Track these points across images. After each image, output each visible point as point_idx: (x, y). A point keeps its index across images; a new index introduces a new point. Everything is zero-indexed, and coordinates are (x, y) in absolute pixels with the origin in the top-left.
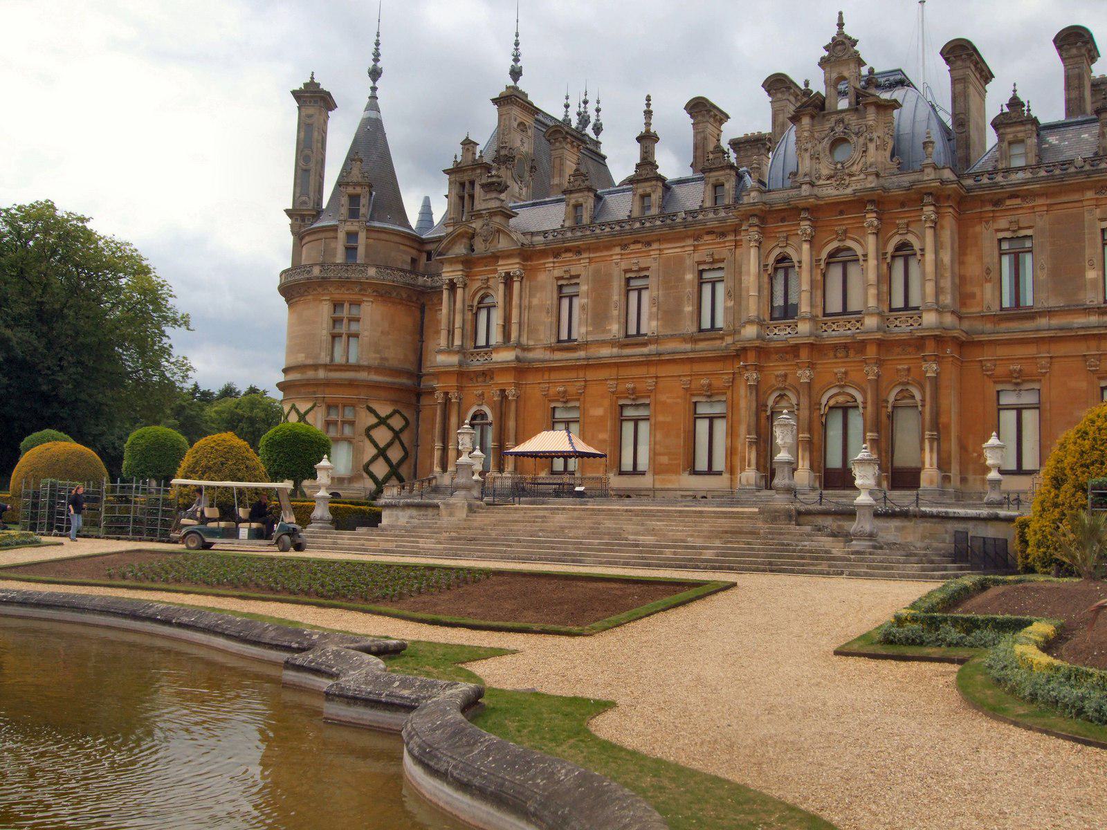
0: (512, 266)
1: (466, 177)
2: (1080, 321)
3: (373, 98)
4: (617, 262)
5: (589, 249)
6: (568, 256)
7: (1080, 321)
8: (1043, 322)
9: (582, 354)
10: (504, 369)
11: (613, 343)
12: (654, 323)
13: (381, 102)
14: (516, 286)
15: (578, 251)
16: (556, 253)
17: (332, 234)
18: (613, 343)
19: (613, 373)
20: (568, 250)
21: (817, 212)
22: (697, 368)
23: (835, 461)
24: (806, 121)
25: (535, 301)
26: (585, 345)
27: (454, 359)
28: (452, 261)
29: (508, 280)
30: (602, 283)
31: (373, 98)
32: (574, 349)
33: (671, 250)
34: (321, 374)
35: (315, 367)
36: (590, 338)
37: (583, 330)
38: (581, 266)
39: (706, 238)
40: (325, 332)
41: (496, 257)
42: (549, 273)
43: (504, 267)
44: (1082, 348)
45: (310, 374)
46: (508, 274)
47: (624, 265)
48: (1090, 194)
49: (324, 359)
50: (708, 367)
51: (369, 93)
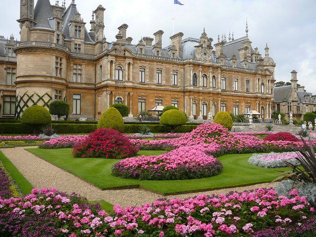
0: (131, 61)
1: (78, 25)
2: (232, 93)
4: (155, 66)
5: (150, 61)
7: (232, 93)
8: (228, 93)
10: (129, 88)
11: (155, 85)
12: (164, 82)
14: (131, 66)
15: (146, 61)
16: (140, 60)
18: (155, 85)
19: (155, 92)
20: (143, 60)
21: (204, 66)
22: (174, 93)
23: (205, 115)
24: (200, 48)
25: (134, 71)
26: (148, 84)
27: (114, 83)
28: (112, 55)
29: (129, 64)
30: (151, 70)
32: (145, 85)
33: (168, 66)
34: (53, 80)
35: (52, 77)
36: (149, 83)
37: (148, 80)
38: (146, 65)
39: (175, 65)
40: (54, 66)
41: (125, 58)
42: (139, 64)
43: (128, 61)
44: (232, 97)
45: (49, 79)
47: (157, 67)
48: (233, 73)
49: (54, 75)
50: (176, 93)
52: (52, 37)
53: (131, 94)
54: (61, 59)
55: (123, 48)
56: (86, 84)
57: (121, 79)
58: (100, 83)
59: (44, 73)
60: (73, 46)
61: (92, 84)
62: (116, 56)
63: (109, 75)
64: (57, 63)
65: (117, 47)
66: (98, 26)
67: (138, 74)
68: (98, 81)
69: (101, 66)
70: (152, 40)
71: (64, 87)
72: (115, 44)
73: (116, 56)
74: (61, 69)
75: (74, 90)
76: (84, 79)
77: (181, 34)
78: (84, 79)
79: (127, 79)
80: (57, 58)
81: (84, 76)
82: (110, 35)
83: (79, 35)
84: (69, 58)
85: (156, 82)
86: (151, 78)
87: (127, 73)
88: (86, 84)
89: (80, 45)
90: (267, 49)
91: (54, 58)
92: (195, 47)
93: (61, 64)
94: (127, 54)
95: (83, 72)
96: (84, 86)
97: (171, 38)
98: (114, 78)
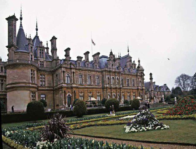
3: (21, 24)
5: (84, 70)
6: (81, 71)
9: (84, 86)
13: (23, 25)
14: (75, 74)
15: (82, 70)
17: (28, 54)
18: (87, 85)
28: (64, 67)
30: (85, 76)
31: (21, 24)
34: (30, 85)
35: (29, 83)
38: (83, 72)
45: (28, 85)
46: (74, 72)
51: (20, 23)
52: (28, 56)
53: (76, 91)
54: (34, 71)
55: (69, 62)
56: (48, 87)
57: (69, 82)
58: (57, 86)
59: (25, 81)
60: (39, 63)
61: (51, 87)
62: (66, 68)
63: (63, 80)
64: (32, 74)
65: (66, 62)
66: (54, 49)
67: (78, 79)
68: (55, 85)
69: (57, 75)
70: (82, 58)
71: (36, 90)
72: (64, 60)
73: (66, 68)
74: (34, 78)
75: (41, 92)
76: (47, 84)
77: (99, 53)
78: (47, 84)
79: (73, 82)
80: (32, 70)
81: (46, 82)
82: (61, 55)
83: (43, 56)
84: (38, 70)
85: (88, 83)
86: (86, 81)
87: (73, 78)
88: (48, 87)
89: (43, 62)
90: (139, 61)
91: (30, 70)
92: (107, 61)
93: (34, 74)
94: (72, 67)
95: (46, 80)
96: (47, 88)
97: (93, 56)
98: (65, 82)
